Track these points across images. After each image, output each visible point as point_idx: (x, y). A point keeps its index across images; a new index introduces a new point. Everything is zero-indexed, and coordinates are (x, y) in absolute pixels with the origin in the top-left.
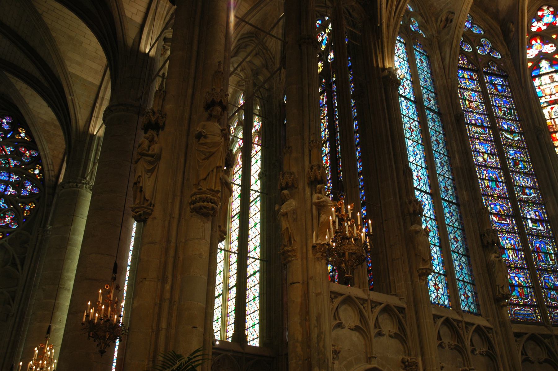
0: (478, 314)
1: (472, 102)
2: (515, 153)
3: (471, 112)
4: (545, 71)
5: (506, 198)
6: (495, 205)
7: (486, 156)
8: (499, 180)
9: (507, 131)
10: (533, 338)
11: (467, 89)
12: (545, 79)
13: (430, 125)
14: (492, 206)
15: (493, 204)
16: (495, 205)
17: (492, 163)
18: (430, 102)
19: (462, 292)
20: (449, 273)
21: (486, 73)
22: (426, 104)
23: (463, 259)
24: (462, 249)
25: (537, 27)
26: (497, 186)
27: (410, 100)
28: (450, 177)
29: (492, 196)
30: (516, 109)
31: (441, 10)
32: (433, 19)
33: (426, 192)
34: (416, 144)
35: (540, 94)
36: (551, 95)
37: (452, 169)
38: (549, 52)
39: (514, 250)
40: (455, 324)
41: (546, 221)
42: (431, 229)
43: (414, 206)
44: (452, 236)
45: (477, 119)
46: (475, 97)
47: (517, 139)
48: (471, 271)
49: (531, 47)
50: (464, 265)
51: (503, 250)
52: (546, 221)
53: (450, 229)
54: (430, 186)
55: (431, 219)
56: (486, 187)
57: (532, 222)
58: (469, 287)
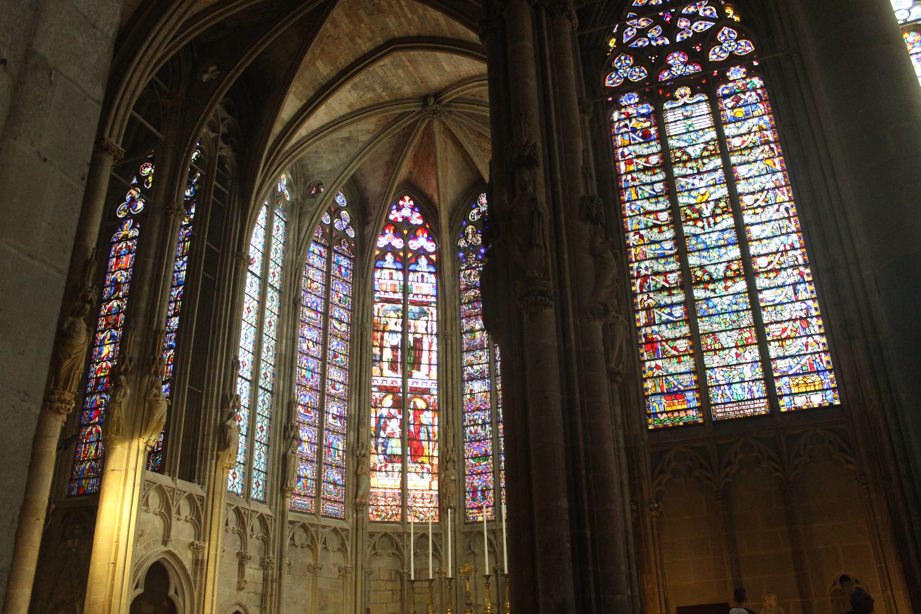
0: (263, 502)
1: (313, 281)
2: (338, 345)
3: (310, 293)
4: (388, 266)
5: (317, 390)
6: (305, 396)
7: (310, 344)
8: (316, 371)
9: (337, 319)
10: (304, 527)
11: (313, 266)
12: (386, 272)
13: (268, 305)
14: (302, 397)
15: (304, 395)
16: (305, 396)
17: (314, 352)
18: (275, 280)
19: (255, 480)
20: (248, 464)
21: (336, 252)
22: (270, 280)
23: (263, 448)
24: (264, 439)
25: (395, 216)
26: (312, 377)
27: (256, 275)
28: (272, 363)
29: (305, 386)
30: (352, 298)
31: (313, 175)
32: (303, 180)
33: (246, 380)
34: (249, 326)
35: (377, 288)
36: (385, 292)
37: (276, 354)
38: (397, 247)
39: (310, 443)
40: (242, 511)
41: (345, 418)
42: (243, 418)
43: (234, 402)
44: (259, 425)
45: (313, 302)
46: (318, 277)
47: (342, 330)
48: (268, 460)
49: (384, 234)
50: (263, 455)
51: (300, 441)
52: (345, 418)
53: (259, 418)
54: (251, 373)
55: (244, 407)
56: (302, 377)
57: (333, 418)
58: (262, 476)
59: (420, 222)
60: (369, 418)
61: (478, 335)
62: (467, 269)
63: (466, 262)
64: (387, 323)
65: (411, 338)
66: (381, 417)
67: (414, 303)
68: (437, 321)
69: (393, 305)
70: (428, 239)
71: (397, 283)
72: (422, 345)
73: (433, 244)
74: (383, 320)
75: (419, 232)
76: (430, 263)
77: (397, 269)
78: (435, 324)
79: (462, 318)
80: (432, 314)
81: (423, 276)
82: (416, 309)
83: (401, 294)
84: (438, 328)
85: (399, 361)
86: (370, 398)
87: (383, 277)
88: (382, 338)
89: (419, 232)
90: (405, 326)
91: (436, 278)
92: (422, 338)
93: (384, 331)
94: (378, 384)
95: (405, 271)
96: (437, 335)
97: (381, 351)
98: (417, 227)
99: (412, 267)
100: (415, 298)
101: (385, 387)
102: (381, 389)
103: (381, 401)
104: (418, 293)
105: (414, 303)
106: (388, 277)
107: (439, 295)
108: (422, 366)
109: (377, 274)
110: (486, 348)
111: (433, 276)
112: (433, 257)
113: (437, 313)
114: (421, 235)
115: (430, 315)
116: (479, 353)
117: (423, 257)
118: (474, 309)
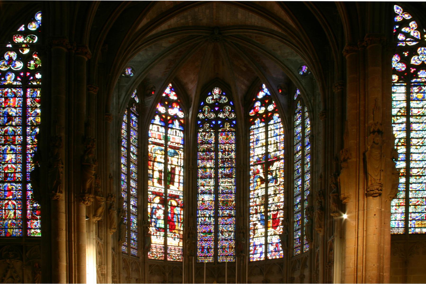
59: (175, 98)
60: (148, 208)
61: (208, 170)
62: (203, 132)
63: (203, 127)
64: (156, 156)
65: (169, 167)
66: (153, 208)
67: (171, 147)
68: (184, 159)
69: (159, 147)
70: (181, 110)
71: (161, 134)
72: (175, 171)
73: (183, 113)
74: (154, 154)
75: (174, 105)
76: (181, 125)
77: (162, 126)
78: (182, 160)
79: (199, 159)
80: (181, 155)
81: (176, 132)
82: (172, 151)
83: (164, 141)
84: (184, 163)
85: (163, 179)
86: (148, 198)
87: (153, 129)
88: (153, 165)
89: (174, 105)
90: (166, 160)
91: (184, 134)
92: (175, 168)
93: (154, 161)
94: (151, 190)
95: (167, 128)
96: (183, 167)
97: (153, 172)
98: (173, 101)
99: (170, 126)
100: (172, 144)
101: (155, 192)
102: (154, 193)
103: (153, 199)
104: (173, 141)
105: (171, 147)
106: (156, 130)
107: (185, 144)
108: (175, 183)
109: (151, 127)
110: (213, 178)
111: (181, 132)
112: (182, 121)
113: (184, 155)
114: (176, 106)
115: (180, 155)
116: (208, 180)
117: (177, 121)
118: (207, 155)
